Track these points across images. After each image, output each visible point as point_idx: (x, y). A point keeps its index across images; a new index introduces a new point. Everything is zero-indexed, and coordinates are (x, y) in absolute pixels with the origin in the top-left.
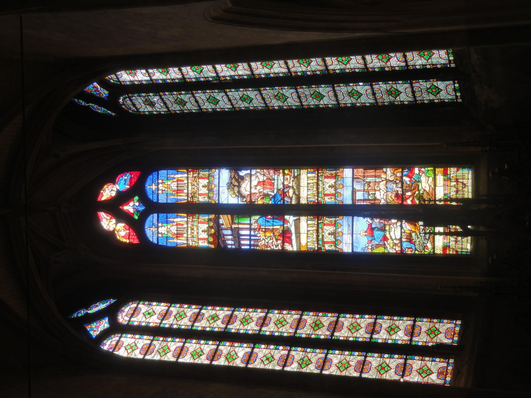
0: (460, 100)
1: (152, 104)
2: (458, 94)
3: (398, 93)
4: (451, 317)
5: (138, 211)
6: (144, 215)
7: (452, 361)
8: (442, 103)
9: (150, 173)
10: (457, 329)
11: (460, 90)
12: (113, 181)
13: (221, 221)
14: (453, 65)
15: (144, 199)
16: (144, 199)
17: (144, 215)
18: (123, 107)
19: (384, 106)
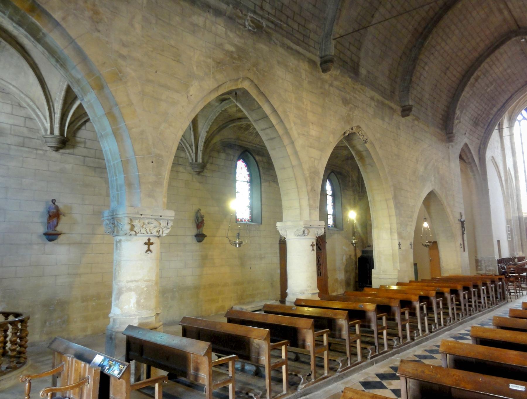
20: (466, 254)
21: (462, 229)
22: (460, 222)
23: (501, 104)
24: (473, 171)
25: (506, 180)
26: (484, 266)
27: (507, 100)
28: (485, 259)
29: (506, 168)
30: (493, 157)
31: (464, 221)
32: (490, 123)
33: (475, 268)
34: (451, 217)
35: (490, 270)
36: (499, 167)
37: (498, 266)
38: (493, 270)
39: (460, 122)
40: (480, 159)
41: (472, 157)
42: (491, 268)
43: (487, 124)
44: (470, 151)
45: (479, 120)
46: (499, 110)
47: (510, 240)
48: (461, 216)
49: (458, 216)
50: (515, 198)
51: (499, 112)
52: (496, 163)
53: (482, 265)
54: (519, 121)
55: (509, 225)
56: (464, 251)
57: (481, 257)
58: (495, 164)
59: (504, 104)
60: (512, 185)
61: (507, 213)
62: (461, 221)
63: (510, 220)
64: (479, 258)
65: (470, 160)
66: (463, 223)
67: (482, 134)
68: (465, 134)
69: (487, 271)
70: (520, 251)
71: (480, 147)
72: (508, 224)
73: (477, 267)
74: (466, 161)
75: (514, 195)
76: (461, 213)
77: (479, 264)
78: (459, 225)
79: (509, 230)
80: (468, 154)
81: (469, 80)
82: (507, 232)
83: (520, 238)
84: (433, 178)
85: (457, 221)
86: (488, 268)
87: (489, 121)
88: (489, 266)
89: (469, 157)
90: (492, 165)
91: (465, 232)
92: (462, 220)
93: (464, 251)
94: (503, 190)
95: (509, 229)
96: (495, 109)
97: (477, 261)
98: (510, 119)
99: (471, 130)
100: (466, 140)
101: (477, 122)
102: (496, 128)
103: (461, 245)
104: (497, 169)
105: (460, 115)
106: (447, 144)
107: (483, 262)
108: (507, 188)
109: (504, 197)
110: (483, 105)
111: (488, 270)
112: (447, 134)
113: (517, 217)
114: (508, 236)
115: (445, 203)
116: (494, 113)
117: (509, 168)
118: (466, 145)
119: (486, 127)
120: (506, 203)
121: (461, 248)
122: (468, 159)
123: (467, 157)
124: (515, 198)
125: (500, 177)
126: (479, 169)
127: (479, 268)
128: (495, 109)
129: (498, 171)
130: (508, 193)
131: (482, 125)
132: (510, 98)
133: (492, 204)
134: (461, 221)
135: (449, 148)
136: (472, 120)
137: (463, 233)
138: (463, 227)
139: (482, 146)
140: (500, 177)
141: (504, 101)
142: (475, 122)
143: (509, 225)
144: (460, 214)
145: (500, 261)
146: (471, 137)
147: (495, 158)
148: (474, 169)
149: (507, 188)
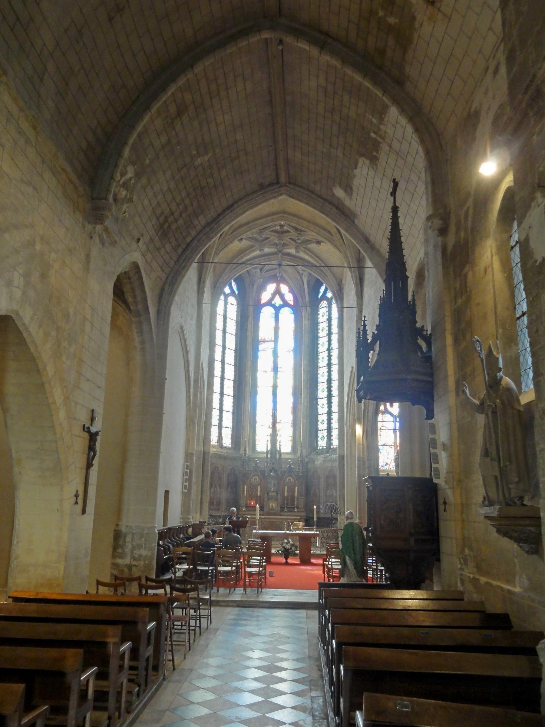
0: (318, 448)
1: (323, 316)
2: (321, 448)
3: (322, 424)
4: (232, 443)
5: (275, 303)
6: (274, 306)
7: (217, 444)
8: (317, 441)
9: (292, 310)
10: (228, 445)
11: (322, 449)
12: (290, 292)
13: (270, 343)
14: (332, 447)
15: (281, 307)
16: (281, 307)
17: (274, 306)
18: (322, 302)
19: (317, 417)
20: (89, 519)
21: (89, 455)
22: (86, 435)
23: (212, 214)
24: (141, 333)
25: (196, 381)
26: (130, 546)
27: (224, 211)
28: (135, 532)
29: (199, 363)
30: (182, 328)
31: (97, 433)
32: (188, 245)
33: (111, 549)
34: (62, 414)
35: (140, 556)
36: (189, 352)
37: (159, 545)
38: (146, 557)
39: (130, 200)
40: (159, 312)
41: (145, 299)
42: (144, 553)
43: (184, 246)
44: (142, 284)
45: (169, 227)
46: (208, 224)
47: (186, 491)
48: (92, 419)
49: (84, 418)
50: (203, 419)
51: (207, 229)
52: (185, 341)
53: (127, 544)
54: (226, 296)
55: (189, 464)
56: (84, 512)
57: (127, 526)
58: (183, 344)
59: (219, 215)
60: (203, 394)
61: (188, 441)
62: (89, 431)
63: (192, 454)
64: (123, 529)
65: (140, 306)
66: (93, 437)
67: (172, 263)
68: (139, 240)
69: (135, 559)
70: (196, 513)
71: (162, 289)
72: (186, 461)
73: (115, 549)
74: (132, 307)
75: (203, 413)
76: (93, 411)
77: (121, 542)
78: (82, 441)
79: (186, 472)
80: (138, 292)
81: (163, 89)
82: (183, 476)
83: (200, 488)
84: (18, 280)
85: (78, 430)
86: (137, 553)
87: (189, 240)
88: (140, 547)
89: (139, 298)
90: (179, 343)
91: (96, 462)
92: (93, 430)
93: (84, 512)
94: (188, 397)
95: (188, 471)
96: (202, 220)
97: (118, 535)
98: (215, 287)
99: (152, 240)
100: (136, 256)
101: (165, 227)
102: (195, 265)
103: (77, 496)
104: (185, 355)
105: (132, 181)
106: (89, 227)
107: (128, 539)
108: (195, 395)
109: (188, 410)
110: (184, 194)
111: (136, 556)
112: (92, 199)
113: (201, 451)
114: (185, 484)
115: (50, 370)
116: (199, 228)
117: (202, 363)
118: (136, 267)
119: (180, 251)
120: (190, 422)
121: (76, 503)
122: (136, 302)
123: (135, 297)
124: (203, 419)
125: (187, 371)
126: (154, 330)
127: (119, 551)
128: (202, 220)
129: (186, 359)
130: (195, 404)
131: (174, 243)
132: (230, 207)
133: (165, 417)
134: (89, 431)
135: (91, 238)
136: (158, 218)
137: (89, 465)
138: (92, 448)
139: (167, 287)
140: (187, 371)
141: (220, 210)
142: (162, 226)
143: (189, 464)
144: (90, 413)
145: (162, 536)
146: (149, 256)
147: (185, 332)
148: (145, 327)
149: (195, 395)
